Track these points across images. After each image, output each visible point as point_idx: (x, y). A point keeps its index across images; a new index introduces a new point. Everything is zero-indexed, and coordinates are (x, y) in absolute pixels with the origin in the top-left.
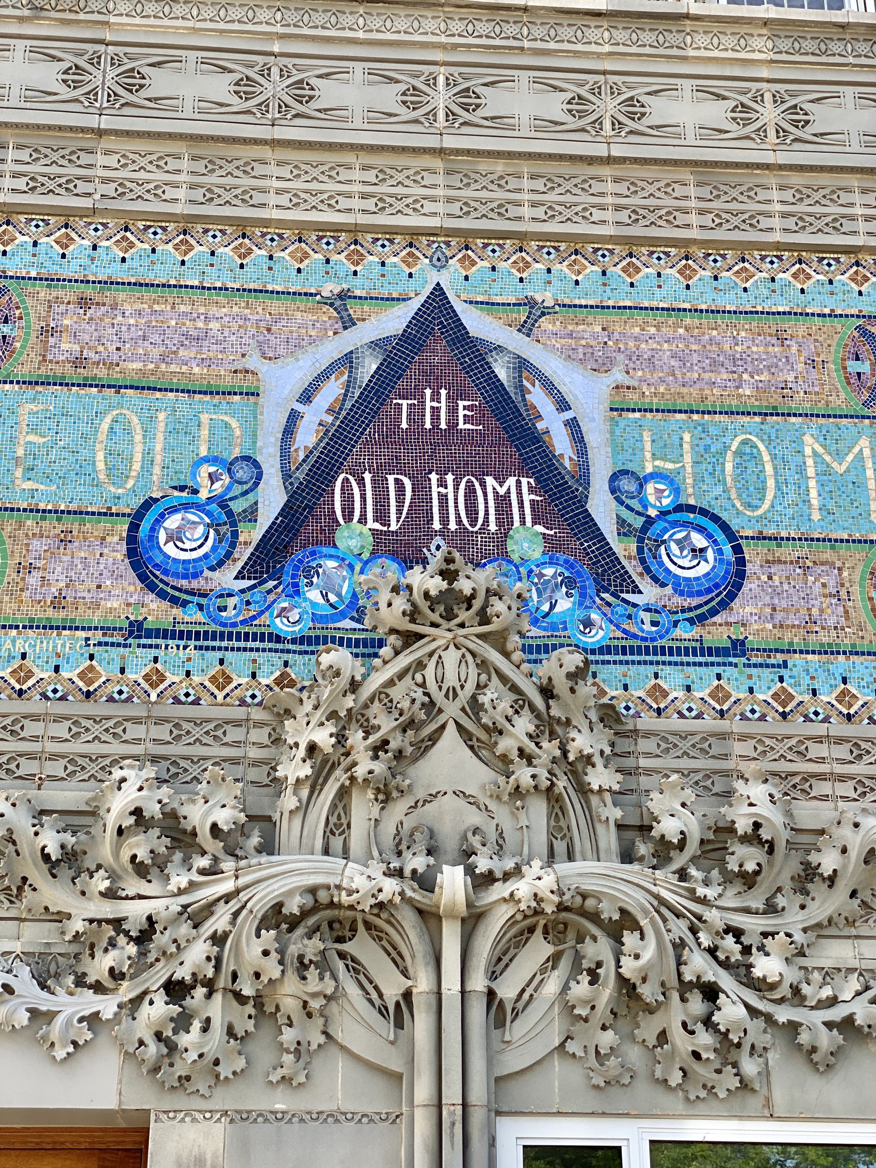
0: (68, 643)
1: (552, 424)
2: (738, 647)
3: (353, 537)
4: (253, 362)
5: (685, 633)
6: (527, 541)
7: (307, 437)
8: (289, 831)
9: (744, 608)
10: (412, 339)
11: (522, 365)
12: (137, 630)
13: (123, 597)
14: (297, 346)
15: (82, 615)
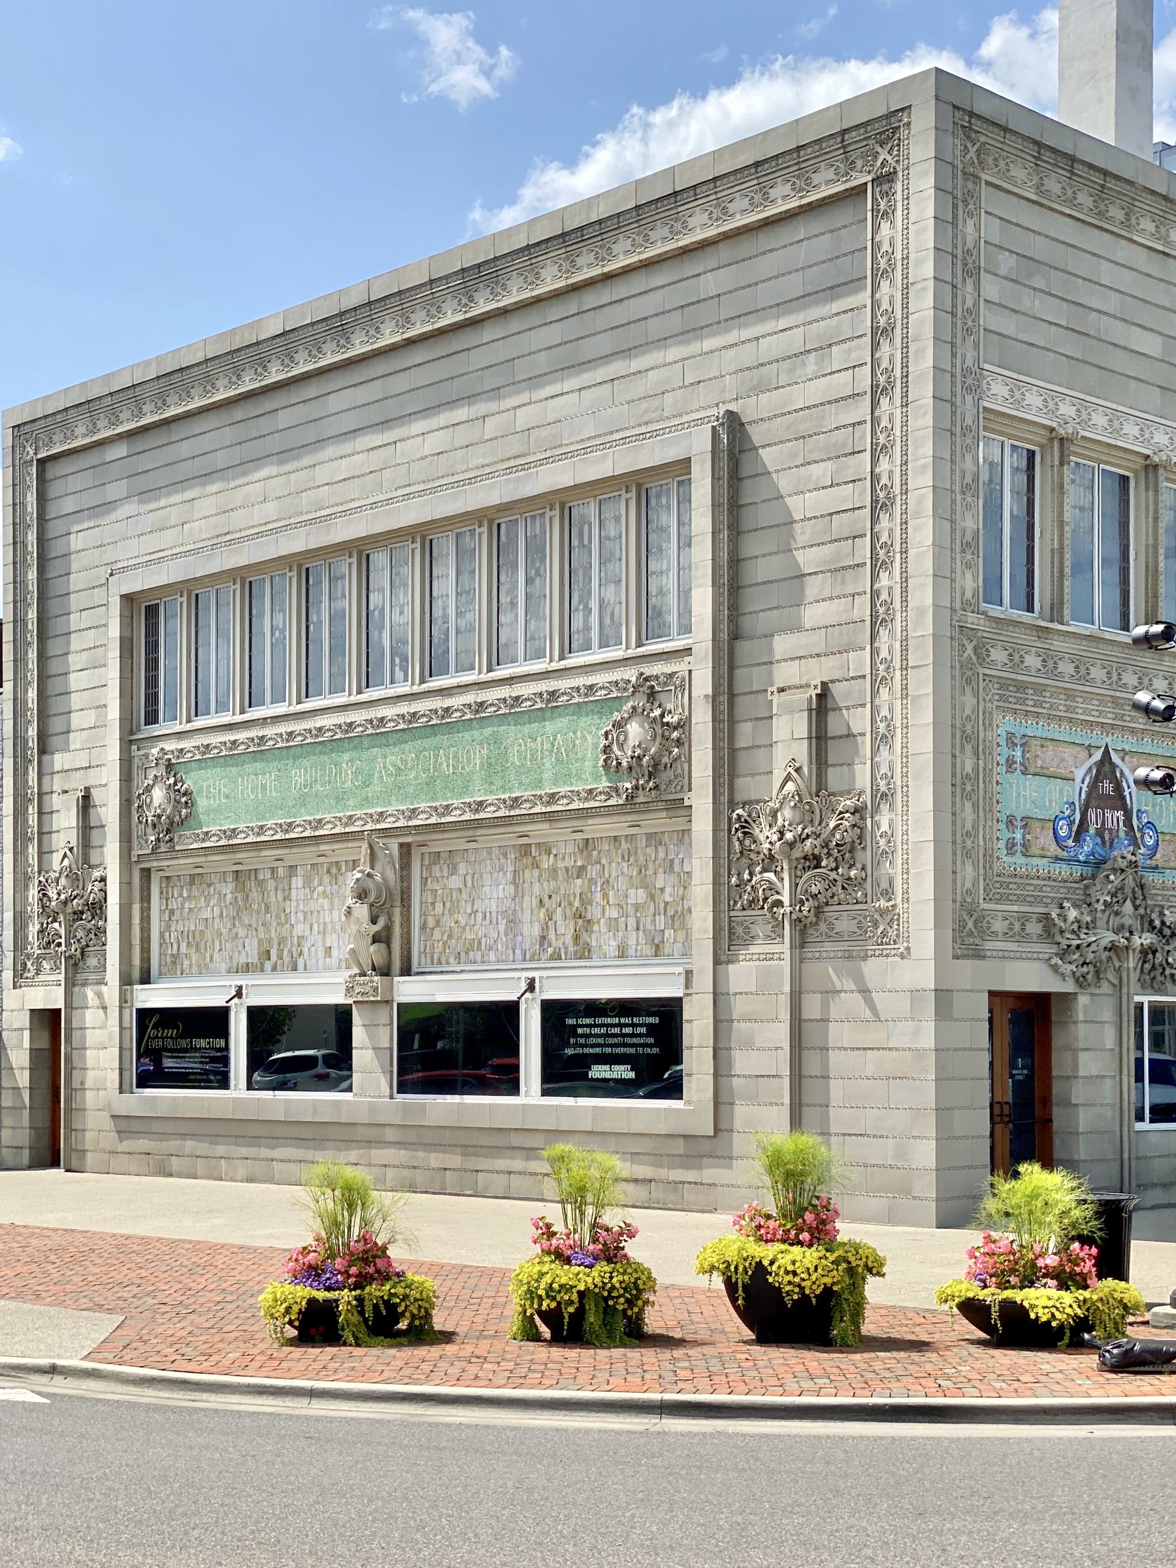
0: (1045, 861)
1: (1126, 793)
2: (1157, 867)
3: (1092, 831)
4: (1073, 769)
5: (1149, 862)
6: (1122, 834)
7: (1083, 796)
8: (1099, 923)
9: (1158, 856)
10: (1100, 764)
11: (1122, 773)
12: (1057, 859)
13: (1054, 849)
14: (1082, 764)
15: (1049, 854)
